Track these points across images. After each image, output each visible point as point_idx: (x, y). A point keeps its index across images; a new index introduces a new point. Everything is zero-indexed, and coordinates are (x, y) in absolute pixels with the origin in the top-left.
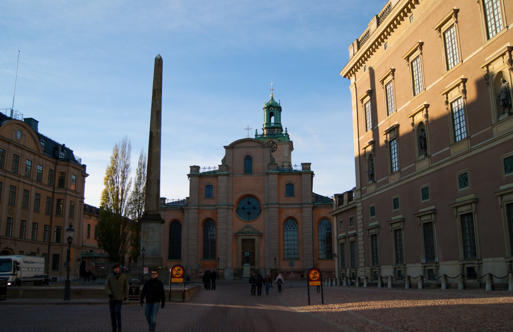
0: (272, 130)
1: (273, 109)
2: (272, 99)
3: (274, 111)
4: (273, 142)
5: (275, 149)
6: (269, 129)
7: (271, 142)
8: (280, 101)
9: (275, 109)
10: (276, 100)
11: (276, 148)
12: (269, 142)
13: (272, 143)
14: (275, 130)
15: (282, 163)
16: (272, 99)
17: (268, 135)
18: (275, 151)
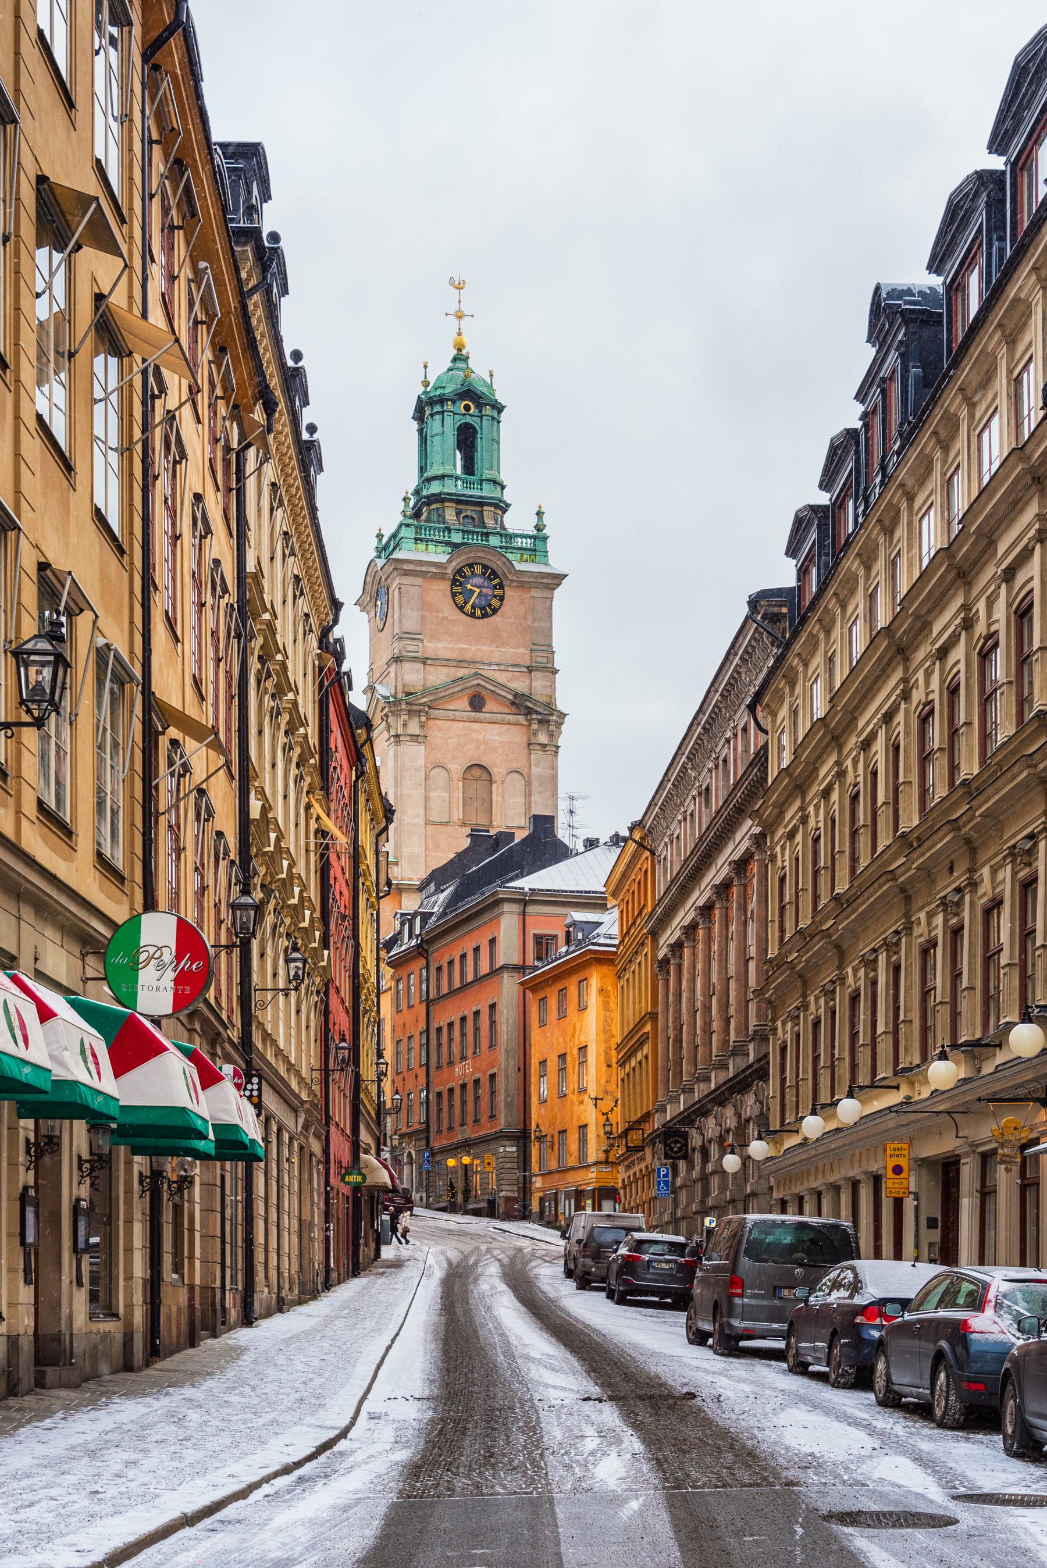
0: (470, 511)
1: (472, 406)
2: (461, 358)
3: (478, 420)
4: (485, 567)
5: (495, 603)
6: (458, 502)
7: (480, 567)
8: (491, 376)
9: (488, 410)
10: (479, 368)
11: (502, 598)
12: (471, 566)
13: (484, 574)
14: (485, 513)
15: (525, 670)
16: (461, 358)
17: (463, 531)
18: (495, 611)
